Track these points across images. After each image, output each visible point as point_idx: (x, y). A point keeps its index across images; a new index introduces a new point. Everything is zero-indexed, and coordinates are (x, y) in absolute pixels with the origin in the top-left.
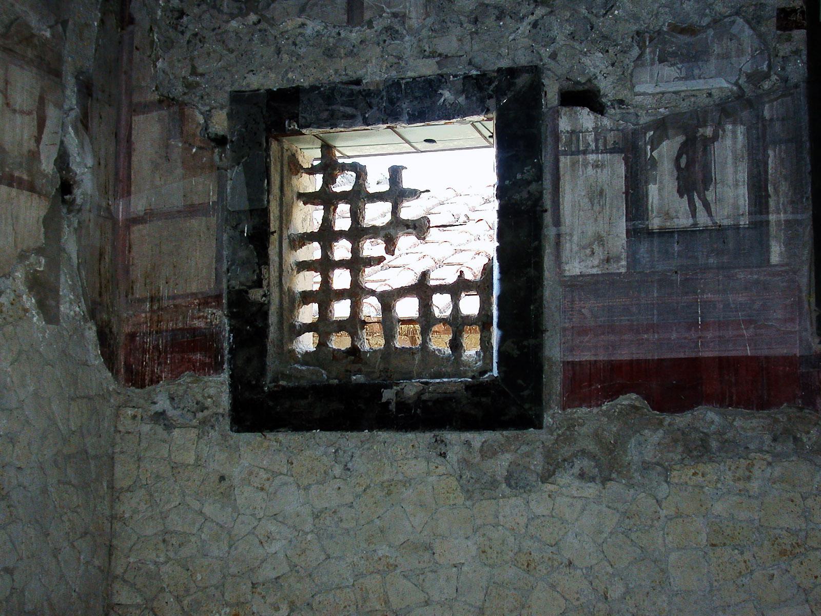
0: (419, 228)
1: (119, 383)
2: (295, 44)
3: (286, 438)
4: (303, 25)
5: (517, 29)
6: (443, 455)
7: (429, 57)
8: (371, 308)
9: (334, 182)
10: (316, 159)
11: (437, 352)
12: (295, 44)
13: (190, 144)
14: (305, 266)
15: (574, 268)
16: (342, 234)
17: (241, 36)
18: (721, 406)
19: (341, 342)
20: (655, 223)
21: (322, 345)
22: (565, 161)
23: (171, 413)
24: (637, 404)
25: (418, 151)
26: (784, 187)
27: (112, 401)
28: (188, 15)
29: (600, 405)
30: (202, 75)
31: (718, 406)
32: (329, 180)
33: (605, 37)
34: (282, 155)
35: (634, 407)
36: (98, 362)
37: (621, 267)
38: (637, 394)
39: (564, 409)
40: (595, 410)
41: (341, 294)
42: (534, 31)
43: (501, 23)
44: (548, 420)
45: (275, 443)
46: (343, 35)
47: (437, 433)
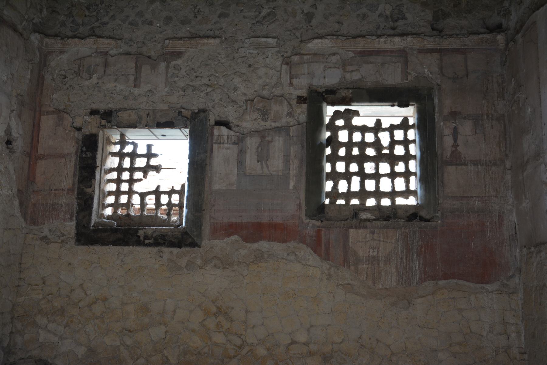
0: (157, 169)
2: (112, 93)
3: (97, 248)
4: (116, 86)
5: (200, 95)
6: (162, 257)
7: (165, 103)
8: (136, 200)
9: (124, 149)
10: (117, 139)
11: (161, 217)
12: (112, 93)
13: (65, 129)
14: (110, 181)
15: (216, 187)
16: (126, 169)
17: (90, 88)
18: (269, 241)
20: (248, 171)
21: (115, 212)
22: (215, 146)
23: (49, 237)
24: (237, 239)
25: (159, 139)
26: (296, 162)
27: (23, 231)
28: (68, 78)
29: (224, 239)
30: (72, 102)
31: (268, 241)
32: (122, 147)
33: (233, 101)
34: (104, 137)
35: (237, 241)
36: (19, 215)
37: (234, 188)
38: (238, 235)
39: (209, 240)
40: (221, 241)
41: (124, 193)
42: (206, 97)
43: (194, 93)
44: (203, 244)
45: (93, 250)
46: (132, 91)
47: (159, 248)
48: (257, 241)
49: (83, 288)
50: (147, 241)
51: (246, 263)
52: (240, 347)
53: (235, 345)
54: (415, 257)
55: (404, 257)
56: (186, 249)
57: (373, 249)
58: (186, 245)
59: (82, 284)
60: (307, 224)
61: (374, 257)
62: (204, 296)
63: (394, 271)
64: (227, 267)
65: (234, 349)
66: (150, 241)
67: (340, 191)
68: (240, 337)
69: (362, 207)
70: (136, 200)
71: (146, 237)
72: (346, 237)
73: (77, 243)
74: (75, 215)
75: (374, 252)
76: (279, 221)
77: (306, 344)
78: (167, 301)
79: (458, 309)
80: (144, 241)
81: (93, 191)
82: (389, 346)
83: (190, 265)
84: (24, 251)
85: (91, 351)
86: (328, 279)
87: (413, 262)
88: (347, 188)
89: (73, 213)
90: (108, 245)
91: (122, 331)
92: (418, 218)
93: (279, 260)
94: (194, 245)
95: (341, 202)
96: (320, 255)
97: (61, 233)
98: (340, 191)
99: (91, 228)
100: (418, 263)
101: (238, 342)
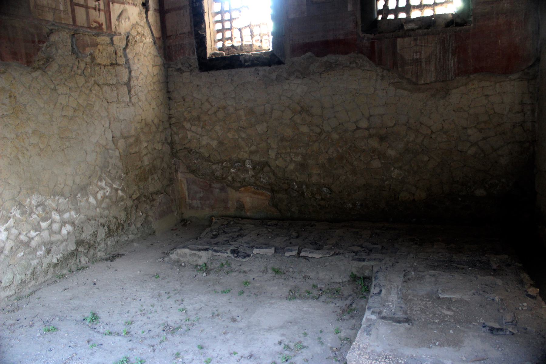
1: (166, 61)
6: (258, 74)
14: (217, 22)
19: (228, 44)
21: (223, 45)
23: (182, 68)
48: (326, 55)
49: (209, 102)
50: (246, 64)
51: (319, 73)
52: (320, 134)
53: (316, 133)
54: (450, 56)
55: (442, 57)
56: (275, 66)
57: (416, 53)
58: (274, 64)
59: (208, 99)
60: (363, 38)
61: (417, 59)
62: (291, 100)
63: (433, 69)
64: (306, 77)
65: (316, 136)
66: (249, 63)
67: (390, 8)
68: (319, 127)
69: (408, 20)
70: (236, 33)
71: (246, 61)
72: (394, 45)
73: (200, 71)
74: (195, 50)
75: (417, 55)
76: (342, 37)
77: (367, 129)
78: (266, 106)
79: (486, 95)
80: (244, 64)
81: (205, 32)
82: (429, 127)
83: (278, 79)
84: (168, 80)
85: (221, 143)
86: (381, 80)
87: (449, 61)
88: (396, 5)
89: (194, 49)
90: (221, 69)
91: (238, 129)
92: (454, 24)
93: (344, 68)
94: (280, 63)
95: (391, 17)
96: (374, 61)
97: (189, 65)
98: (390, 8)
99: (208, 58)
100: (453, 61)
101: (318, 130)
